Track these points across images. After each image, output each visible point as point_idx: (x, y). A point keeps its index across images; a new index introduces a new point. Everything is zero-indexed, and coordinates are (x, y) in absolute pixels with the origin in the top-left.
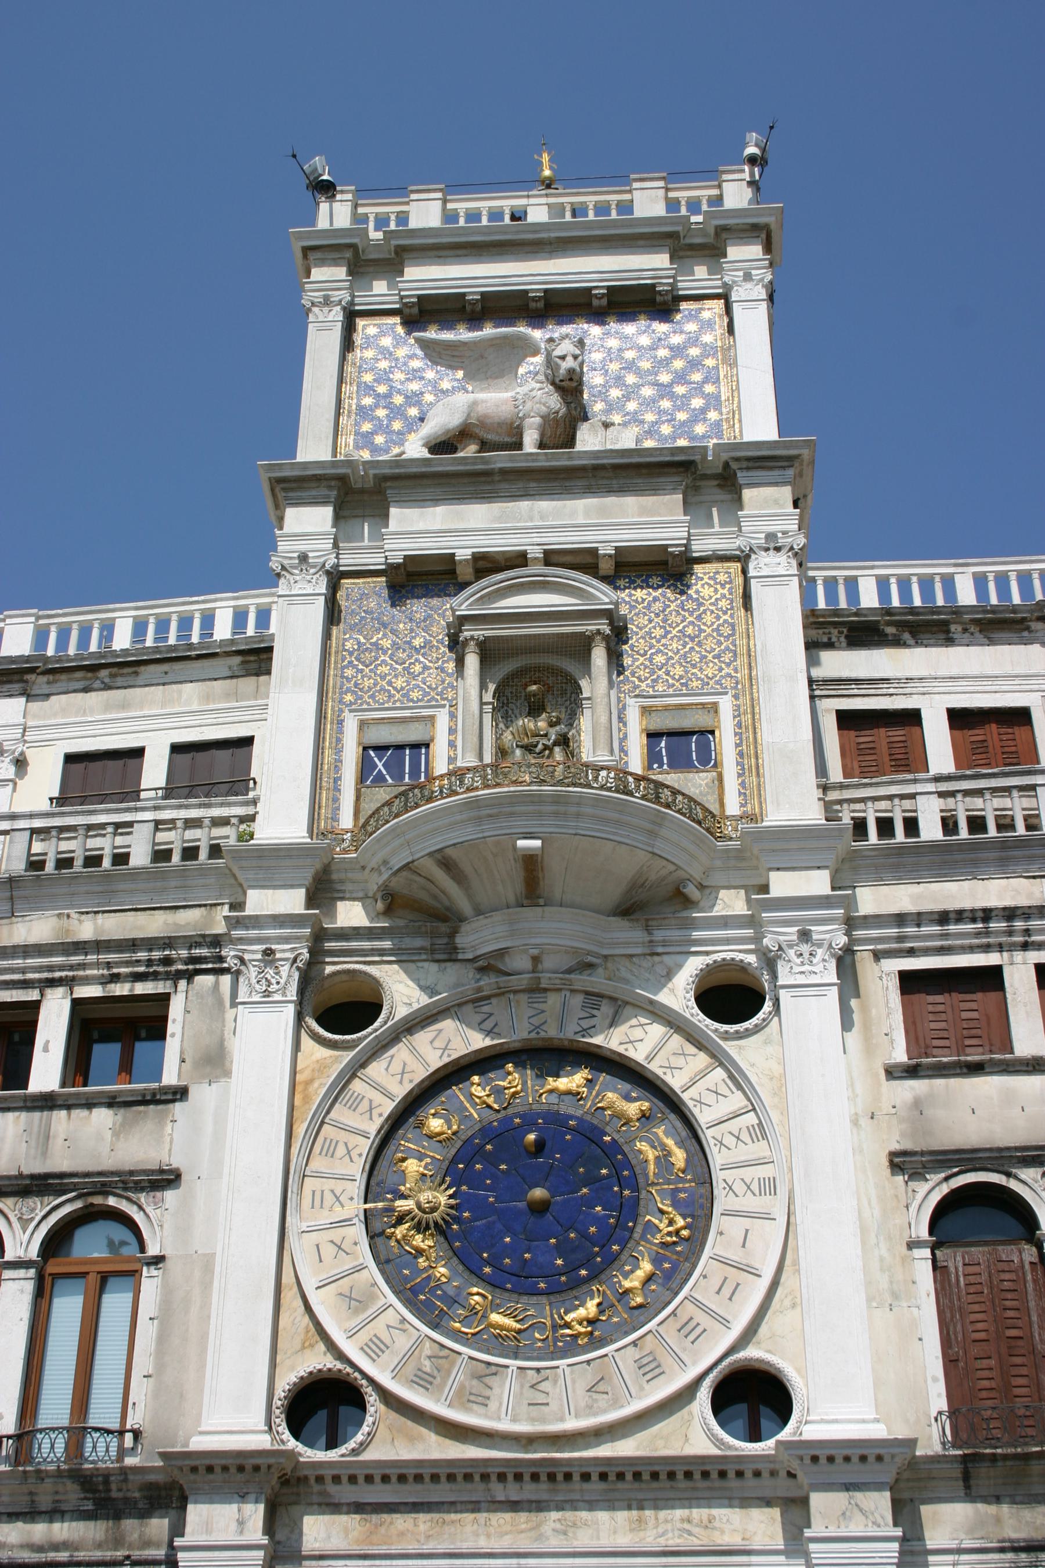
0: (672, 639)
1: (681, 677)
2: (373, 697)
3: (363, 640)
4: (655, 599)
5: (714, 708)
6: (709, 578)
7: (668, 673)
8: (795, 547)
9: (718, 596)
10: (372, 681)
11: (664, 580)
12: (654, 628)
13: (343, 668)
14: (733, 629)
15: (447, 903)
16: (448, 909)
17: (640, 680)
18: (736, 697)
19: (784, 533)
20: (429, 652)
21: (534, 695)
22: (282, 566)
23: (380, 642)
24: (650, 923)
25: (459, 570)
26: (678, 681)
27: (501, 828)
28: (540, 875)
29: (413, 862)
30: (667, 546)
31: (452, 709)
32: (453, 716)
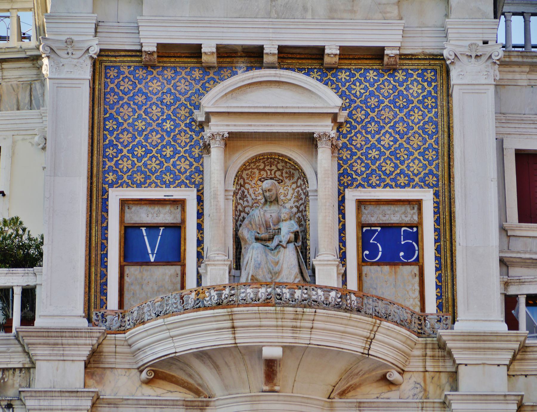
0: (384, 134)
1: (391, 173)
2: (130, 178)
3: (121, 121)
4: (372, 94)
5: (419, 203)
6: (419, 75)
7: (380, 167)
8: (493, 57)
9: (425, 93)
10: (130, 162)
11: (380, 75)
12: (369, 122)
13: (106, 147)
14: (437, 127)
15: (200, 382)
16: (199, 385)
17: (357, 174)
18: (436, 194)
19: (485, 43)
20: (178, 136)
21: (269, 190)
22: (51, 49)
23: (136, 123)
24: (362, 405)
25: (204, 58)
26: (388, 176)
27: (251, 337)
28: (278, 370)
29: (176, 353)
30: (383, 49)
31: (199, 193)
32: (200, 200)
